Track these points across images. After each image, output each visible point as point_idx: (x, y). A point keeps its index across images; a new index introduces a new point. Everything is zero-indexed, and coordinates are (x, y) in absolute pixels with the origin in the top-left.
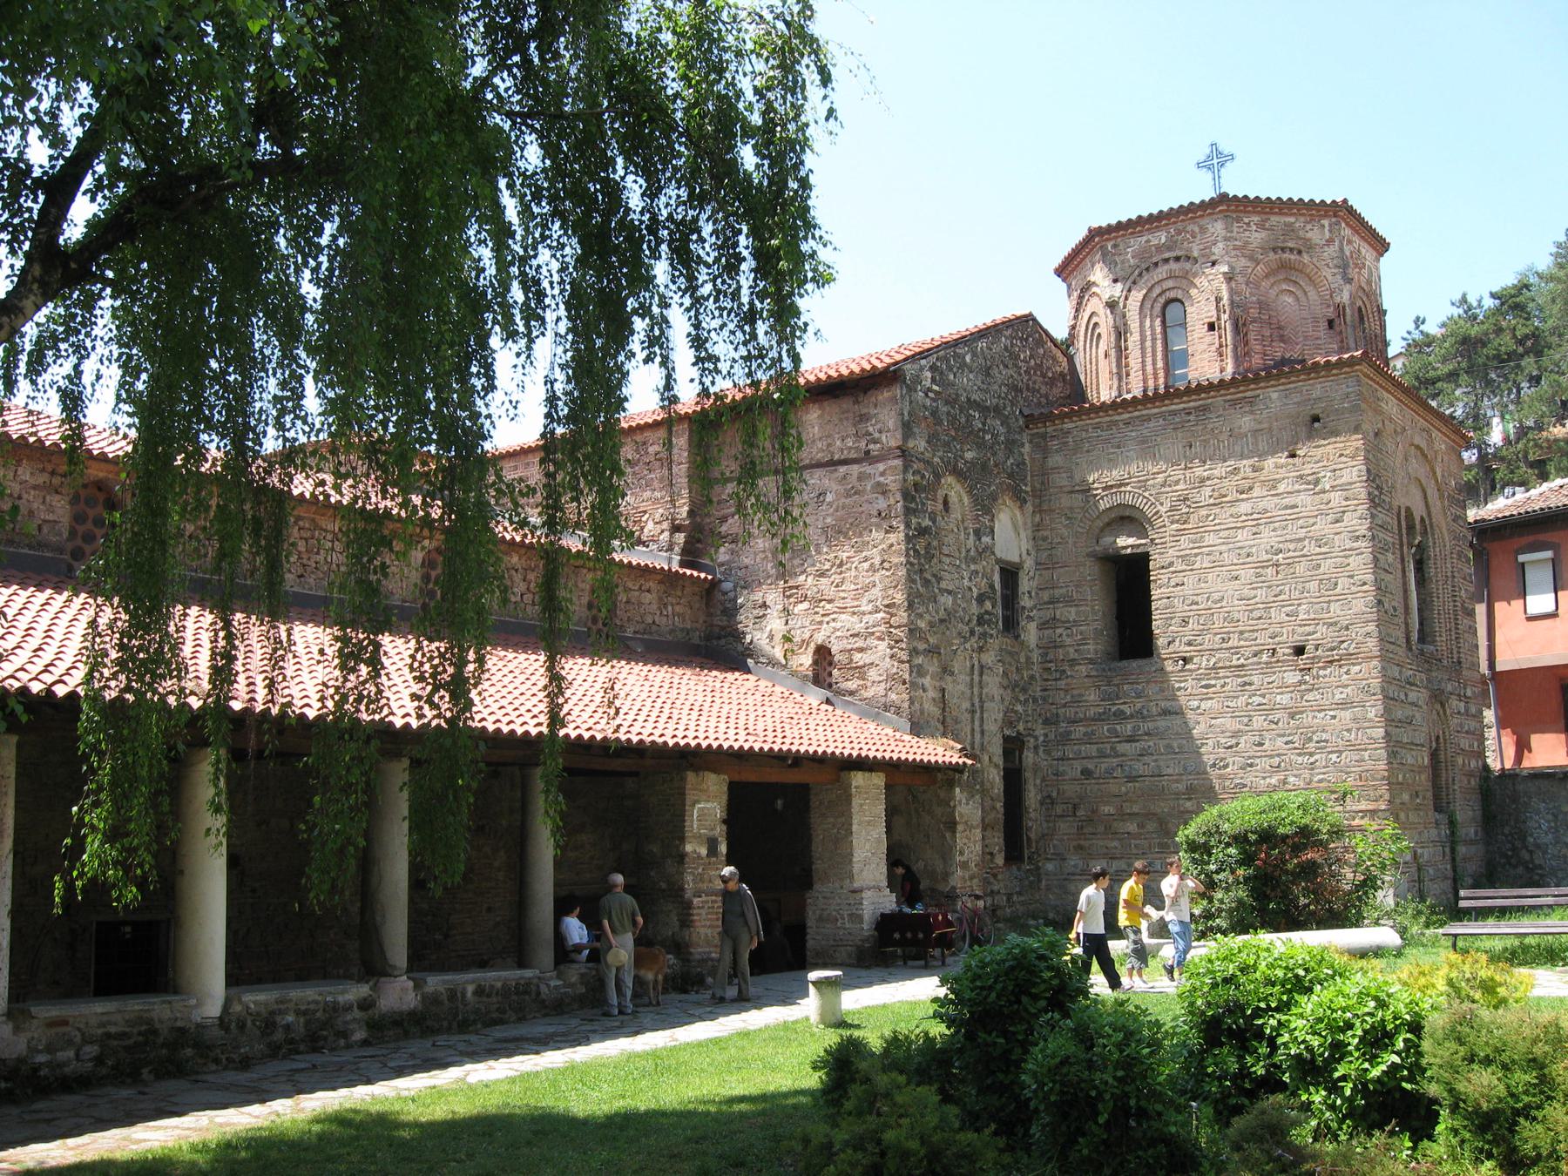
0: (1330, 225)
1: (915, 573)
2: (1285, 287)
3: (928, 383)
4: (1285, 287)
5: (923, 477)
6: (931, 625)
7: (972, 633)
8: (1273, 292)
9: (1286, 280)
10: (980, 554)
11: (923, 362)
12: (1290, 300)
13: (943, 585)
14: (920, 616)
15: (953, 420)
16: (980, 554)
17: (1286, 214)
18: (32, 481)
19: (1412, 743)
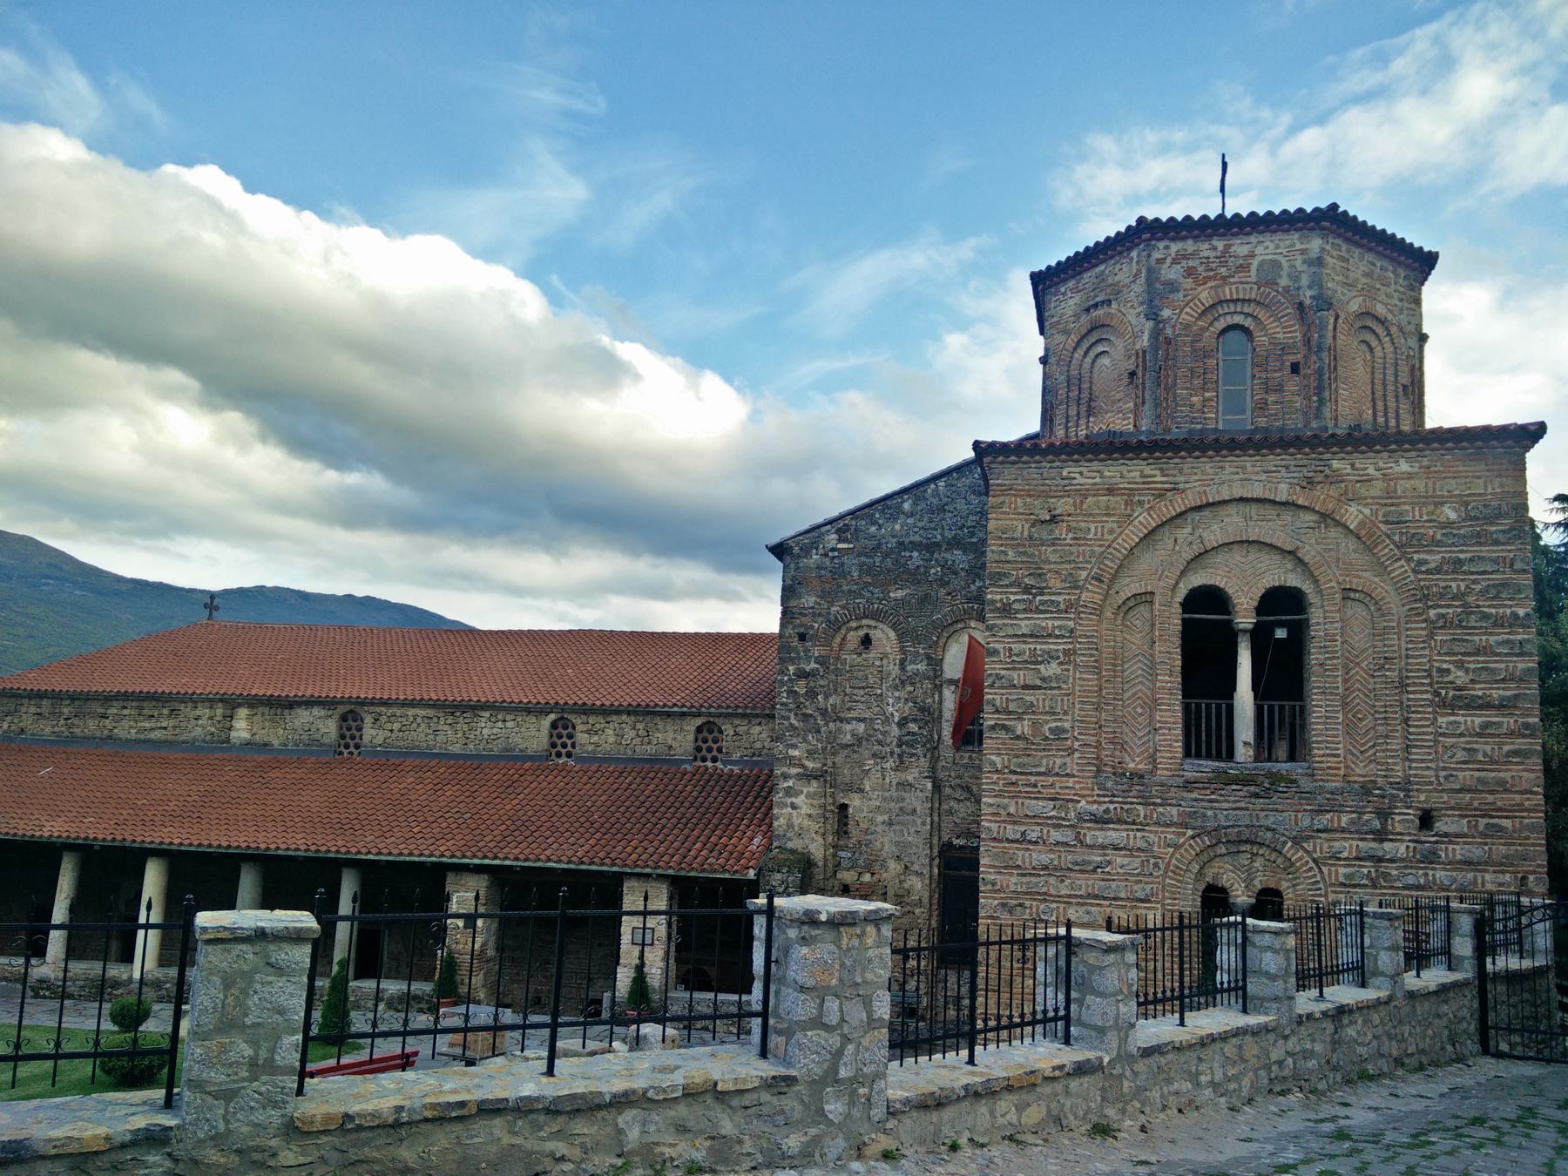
0: (1138, 255)
1: (790, 711)
2: (1100, 348)
3: (832, 544)
4: (1100, 348)
5: (812, 627)
6: (811, 754)
7: (892, 753)
8: (1088, 360)
9: (1099, 341)
10: (903, 683)
11: (824, 529)
12: (1105, 361)
13: (853, 714)
14: (794, 746)
15: (867, 570)
16: (903, 683)
17: (1096, 265)
18: (319, 715)
19: (1089, 896)
